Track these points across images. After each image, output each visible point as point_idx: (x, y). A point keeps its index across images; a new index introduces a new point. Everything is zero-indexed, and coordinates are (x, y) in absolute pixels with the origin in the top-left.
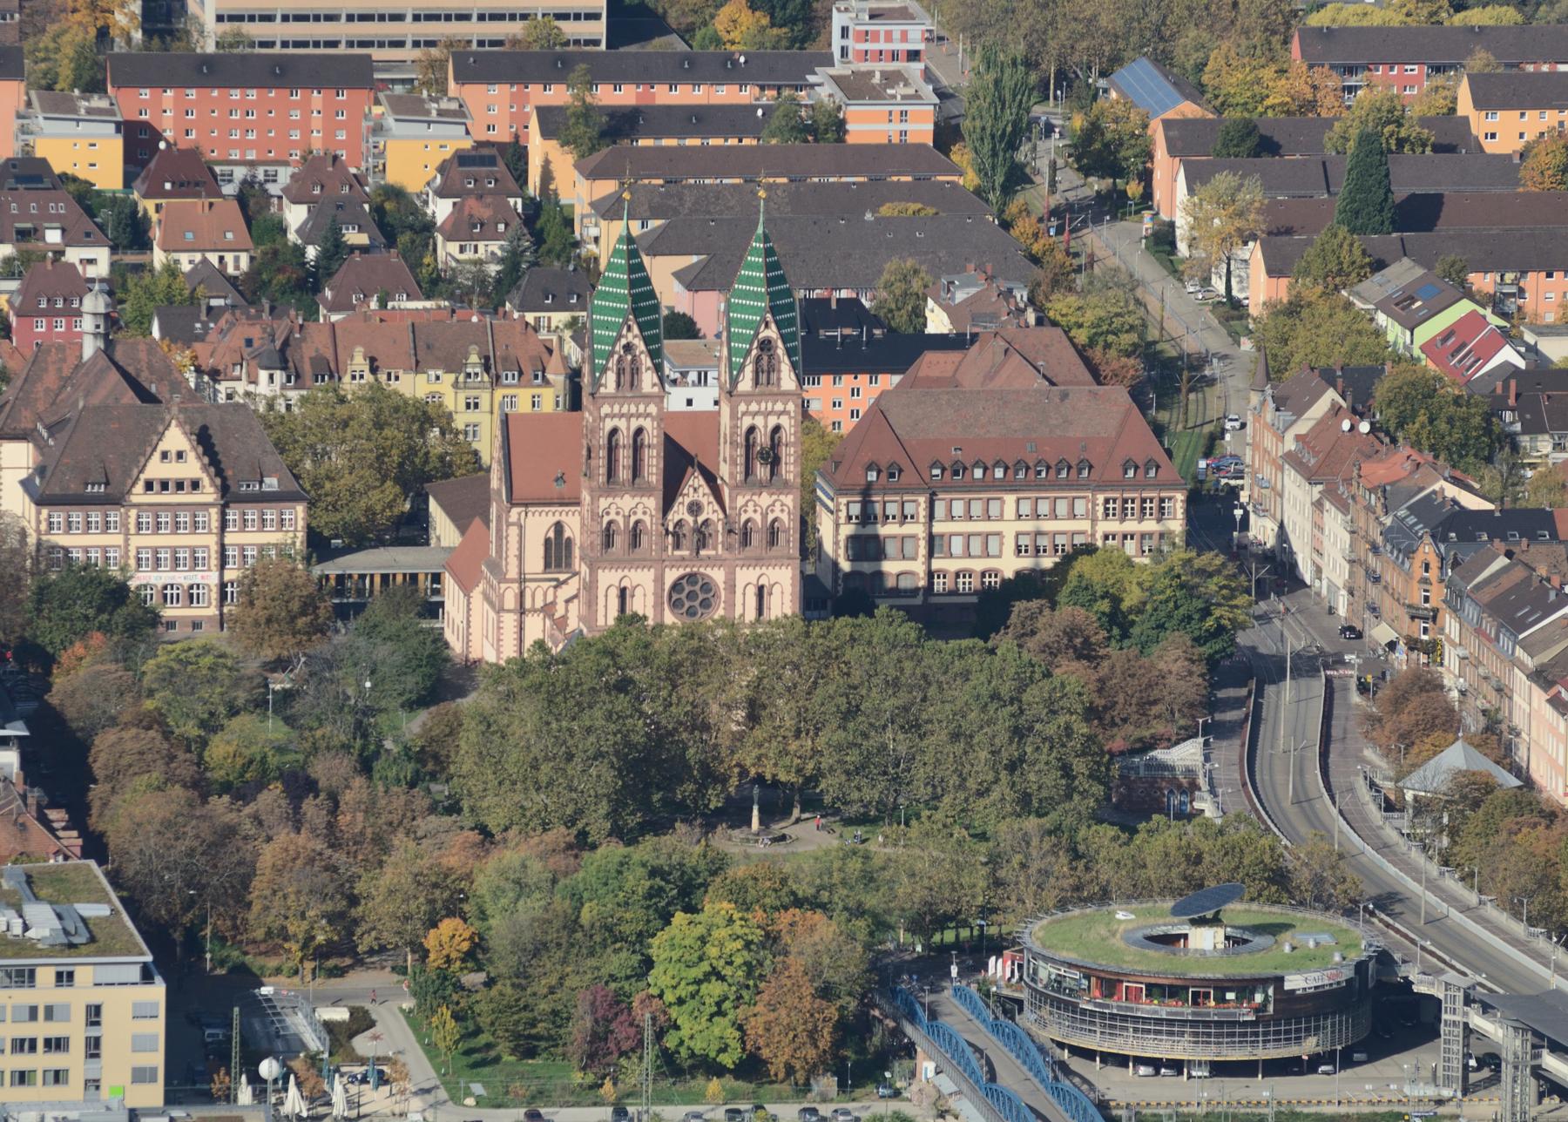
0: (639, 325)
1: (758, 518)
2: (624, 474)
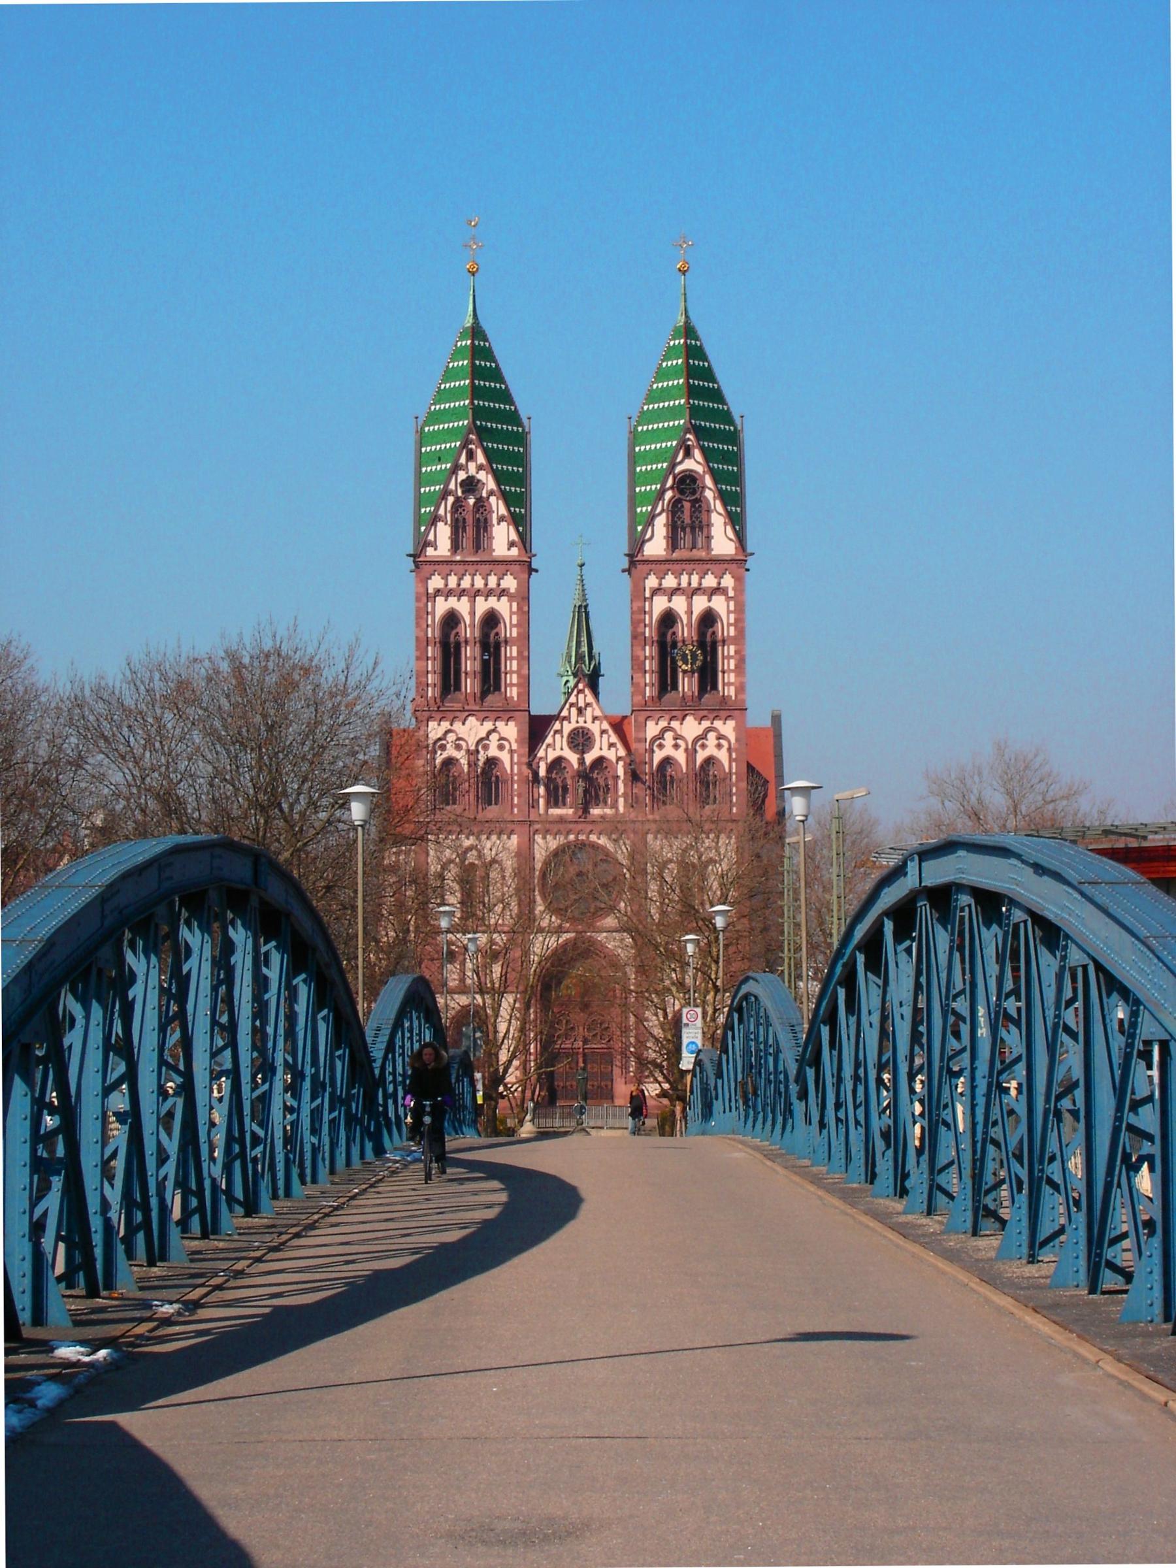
0: (486, 451)
1: (680, 756)
2: (470, 685)
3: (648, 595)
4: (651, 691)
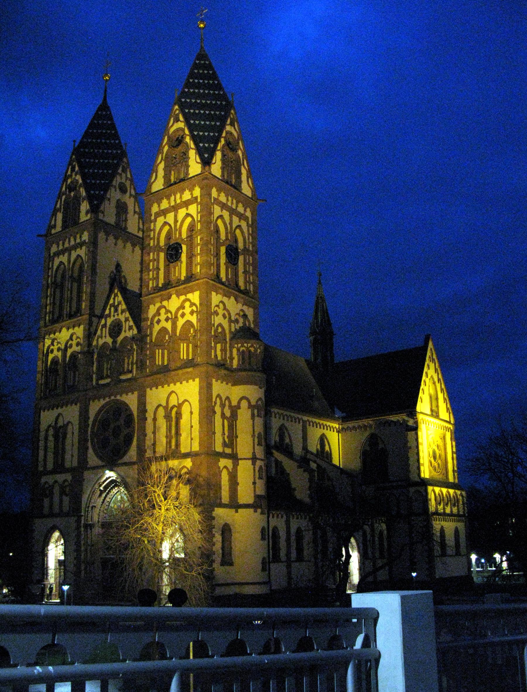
3: (153, 218)
4: (153, 284)
